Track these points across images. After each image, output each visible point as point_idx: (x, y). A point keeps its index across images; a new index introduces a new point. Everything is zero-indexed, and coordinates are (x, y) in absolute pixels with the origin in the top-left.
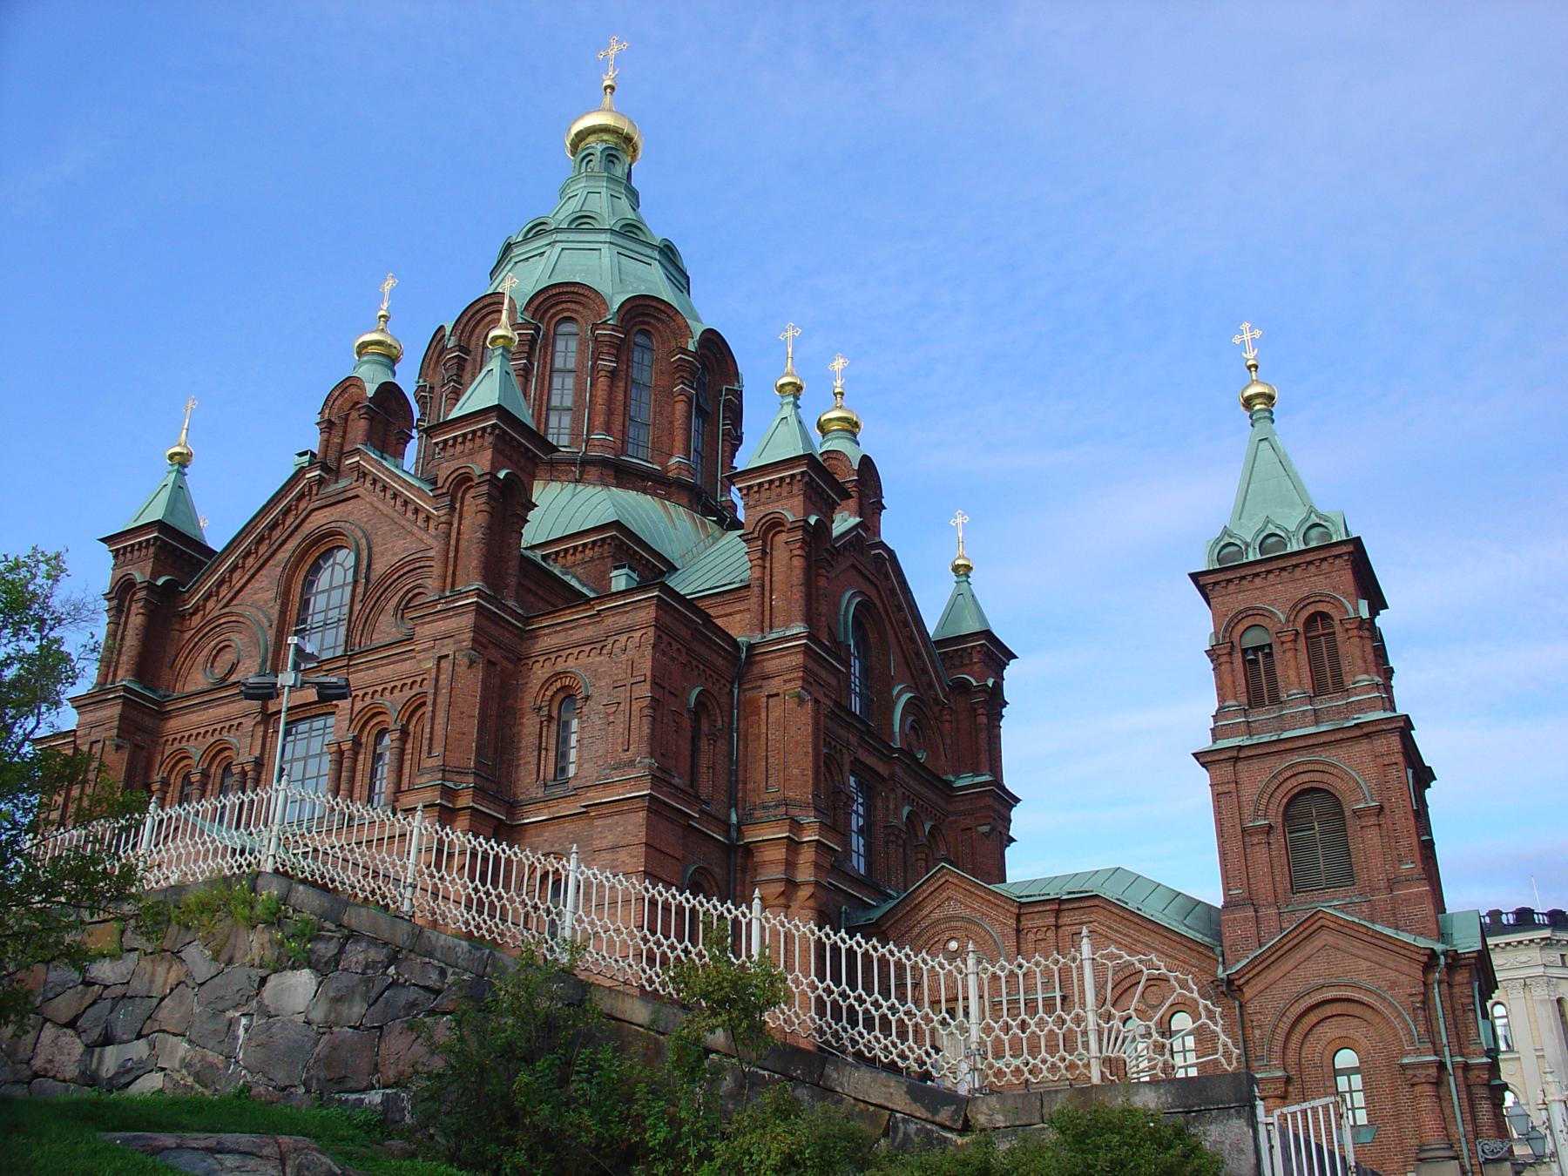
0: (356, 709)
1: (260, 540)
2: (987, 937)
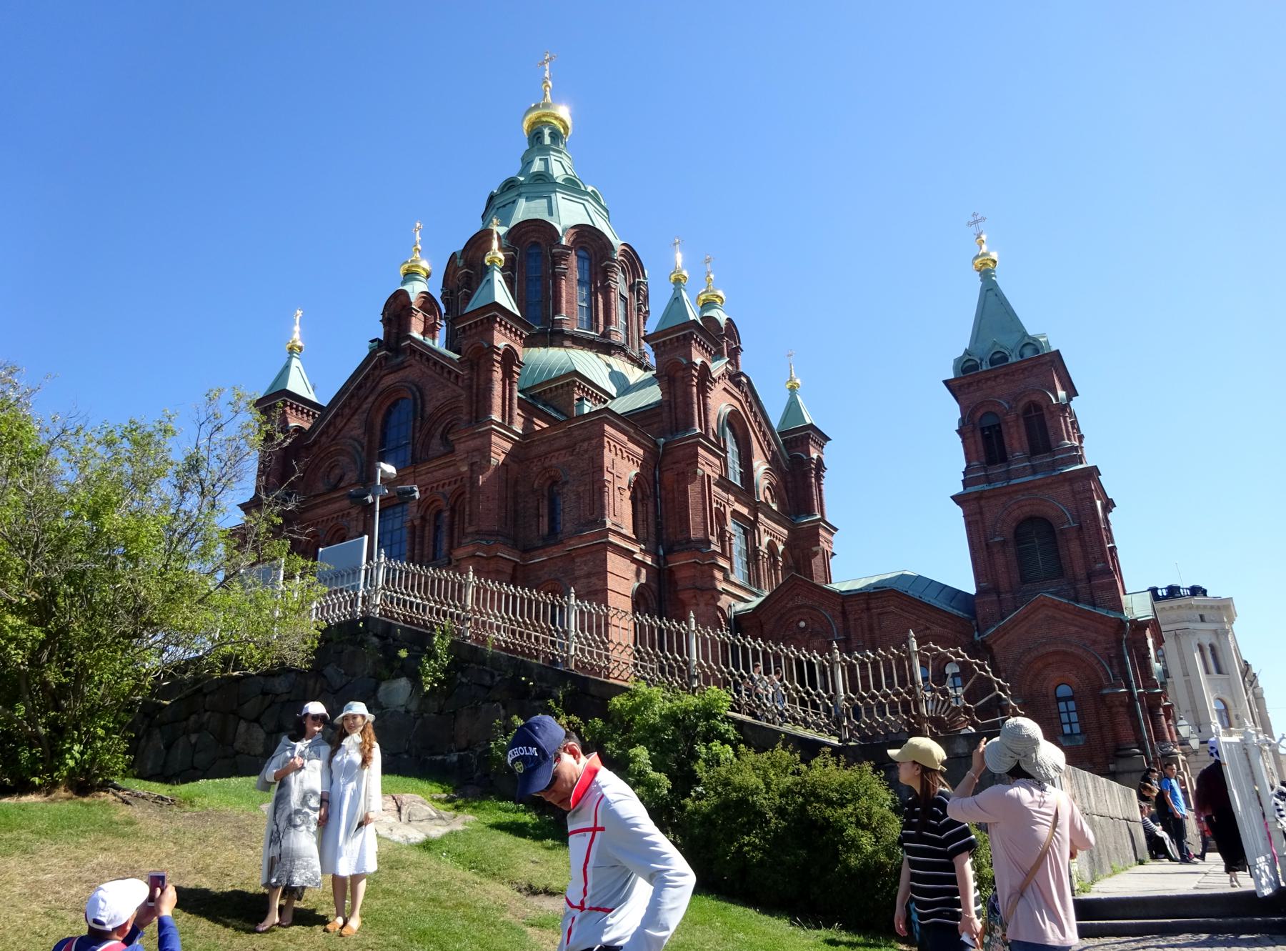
1: (352, 396)
2: (823, 618)
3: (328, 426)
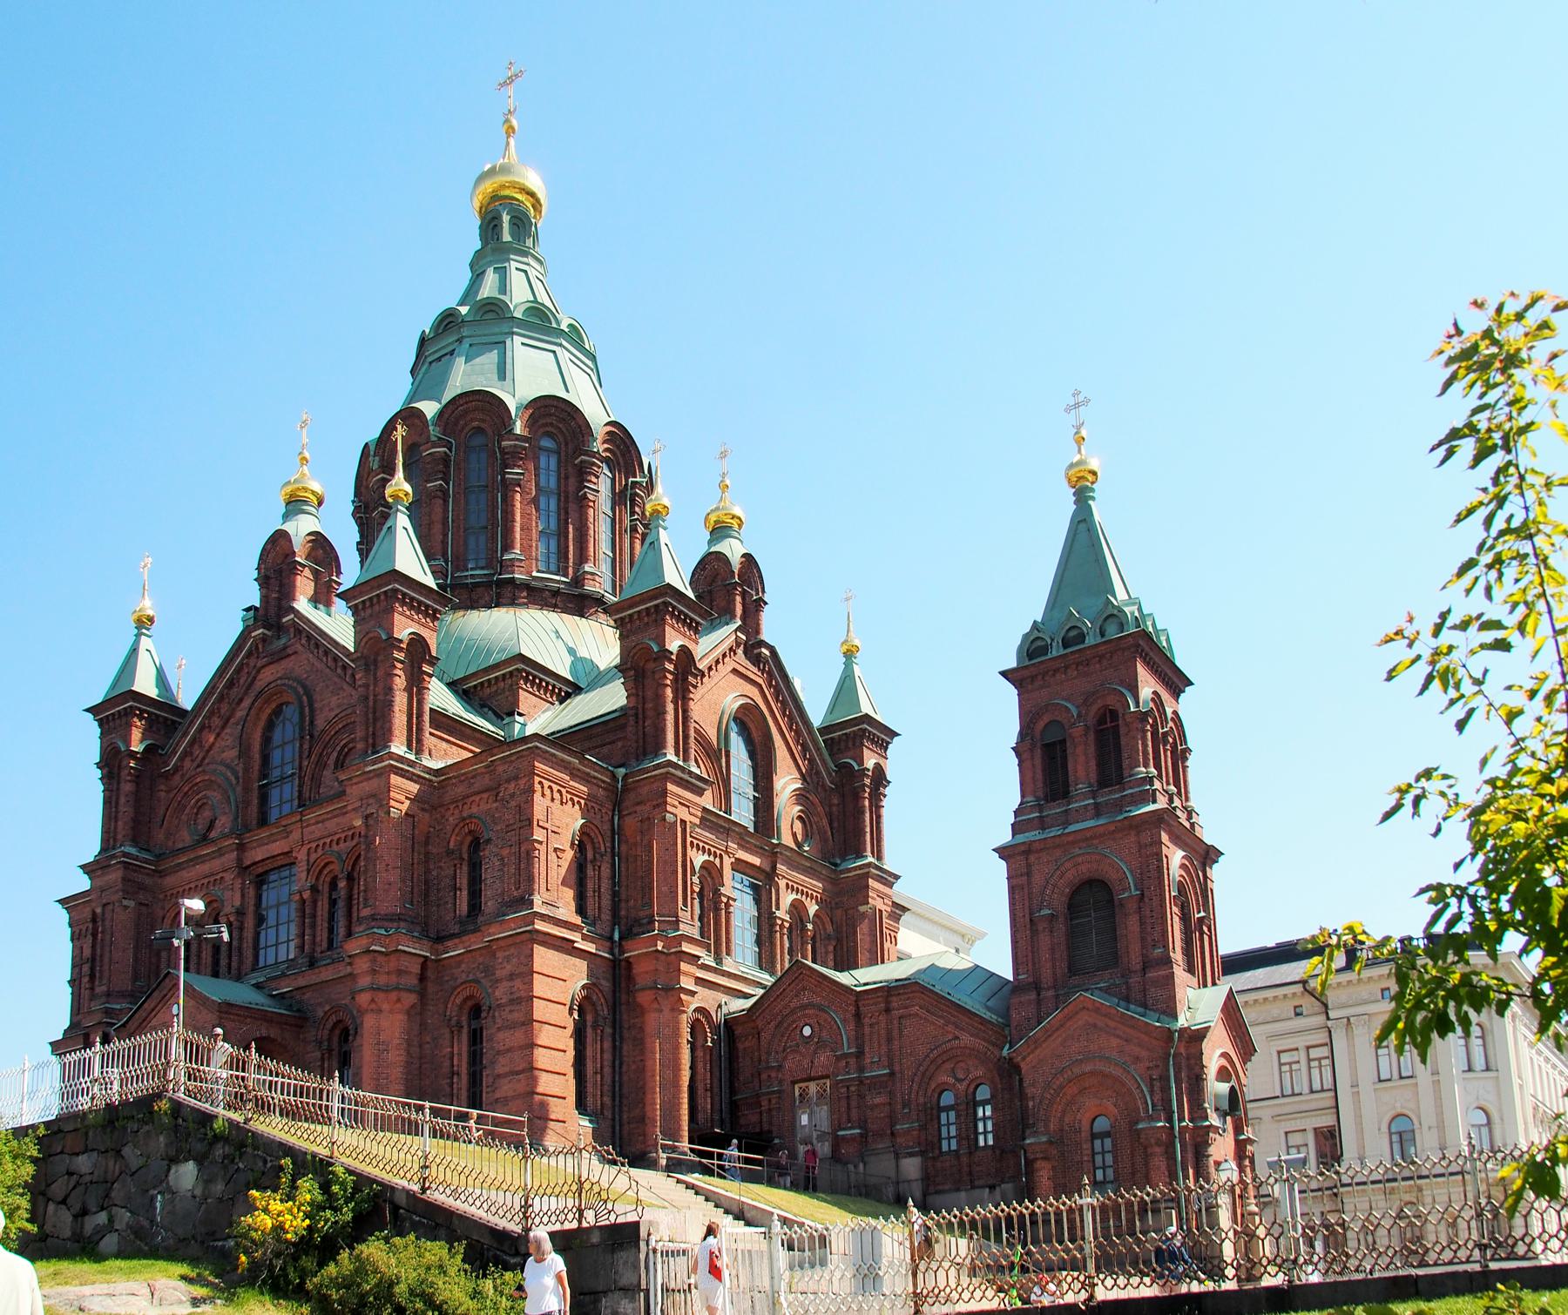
0: (312, 861)
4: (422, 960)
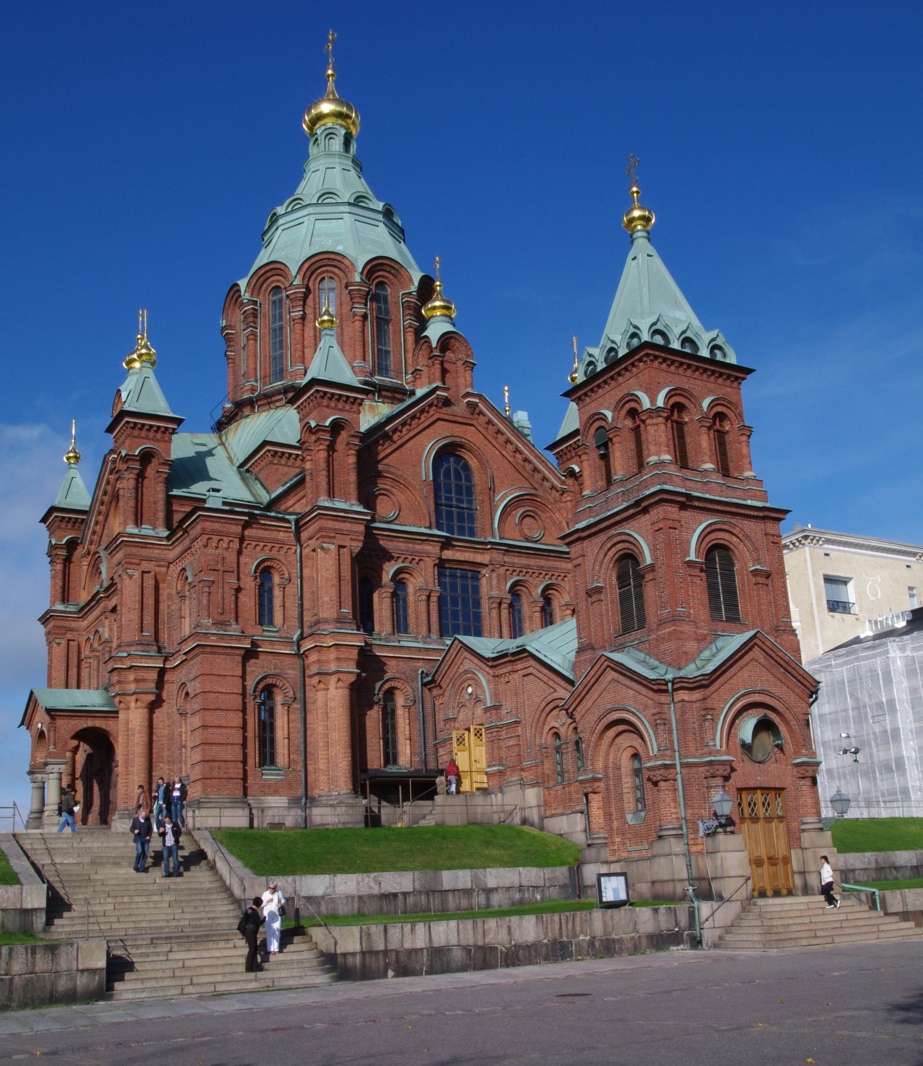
3: (94, 533)
4: (158, 669)
